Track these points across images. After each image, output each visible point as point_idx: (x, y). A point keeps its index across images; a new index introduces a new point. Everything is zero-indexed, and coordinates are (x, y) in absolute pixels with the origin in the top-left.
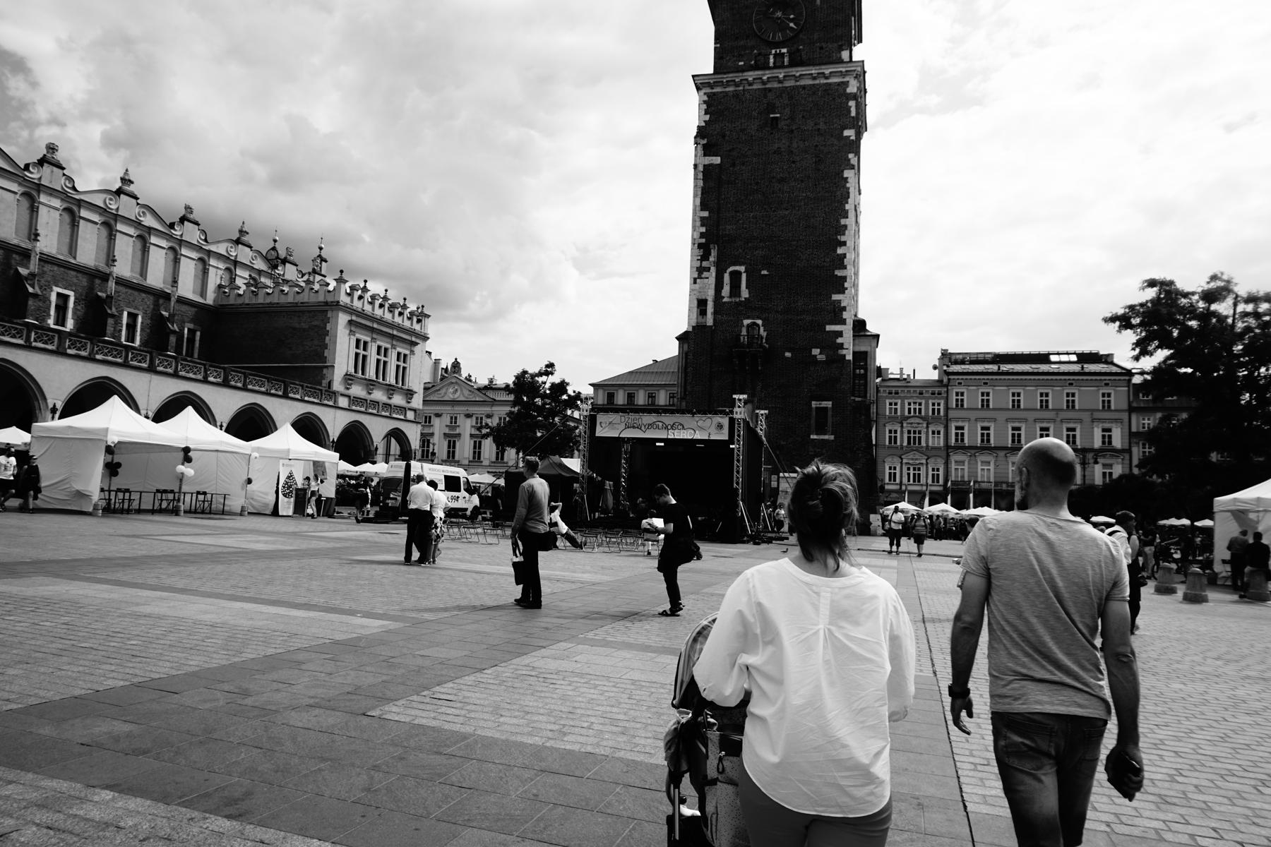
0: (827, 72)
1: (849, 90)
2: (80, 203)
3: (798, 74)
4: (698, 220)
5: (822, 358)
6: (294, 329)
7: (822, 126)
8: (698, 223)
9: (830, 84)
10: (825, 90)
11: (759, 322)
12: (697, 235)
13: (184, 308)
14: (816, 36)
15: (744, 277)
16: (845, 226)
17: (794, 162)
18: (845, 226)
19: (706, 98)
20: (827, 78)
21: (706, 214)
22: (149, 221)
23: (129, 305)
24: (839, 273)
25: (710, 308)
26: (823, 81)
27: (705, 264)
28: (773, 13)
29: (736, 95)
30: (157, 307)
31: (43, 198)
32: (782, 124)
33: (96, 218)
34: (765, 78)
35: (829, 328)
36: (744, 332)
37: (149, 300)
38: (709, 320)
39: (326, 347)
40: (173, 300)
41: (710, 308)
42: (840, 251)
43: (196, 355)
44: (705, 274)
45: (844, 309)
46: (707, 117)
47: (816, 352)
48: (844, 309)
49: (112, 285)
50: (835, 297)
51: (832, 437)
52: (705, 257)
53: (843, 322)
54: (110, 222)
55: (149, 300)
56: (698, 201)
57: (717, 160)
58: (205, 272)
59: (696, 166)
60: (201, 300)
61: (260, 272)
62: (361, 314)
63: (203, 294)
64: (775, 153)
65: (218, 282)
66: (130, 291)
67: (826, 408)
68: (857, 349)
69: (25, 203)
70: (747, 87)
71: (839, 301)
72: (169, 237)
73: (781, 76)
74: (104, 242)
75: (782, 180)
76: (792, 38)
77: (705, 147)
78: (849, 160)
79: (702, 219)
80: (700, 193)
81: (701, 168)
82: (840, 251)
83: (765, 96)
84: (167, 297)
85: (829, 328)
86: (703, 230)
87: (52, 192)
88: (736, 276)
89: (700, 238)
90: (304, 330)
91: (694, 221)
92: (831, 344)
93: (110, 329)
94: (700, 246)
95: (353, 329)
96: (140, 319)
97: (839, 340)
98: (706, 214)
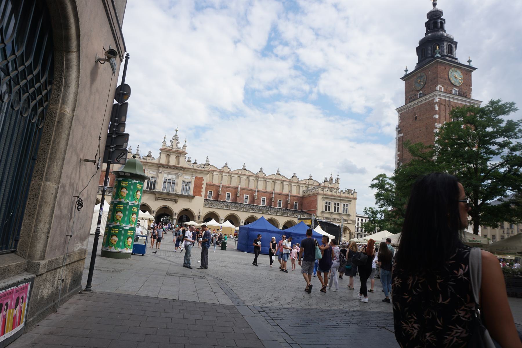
0: (428, 97)
1: (435, 101)
2: (267, 178)
3: (420, 101)
4: (397, 155)
6: (313, 200)
7: (428, 116)
8: (397, 156)
9: (429, 101)
10: (429, 103)
12: (397, 160)
13: (294, 198)
14: (429, 84)
17: (421, 130)
19: (400, 115)
20: (428, 99)
21: (399, 153)
22: (283, 179)
23: (279, 199)
26: (428, 100)
28: (418, 80)
29: (407, 112)
30: (286, 198)
31: (259, 179)
32: (418, 118)
33: (271, 181)
34: (412, 104)
37: (284, 197)
39: (316, 204)
40: (290, 196)
43: (297, 209)
46: (400, 122)
49: (274, 195)
54: (274, 181)
55: (284, 197)
56: (397, 149)
57: (402, 135)
58: (299, 188)
59: (396, 138)
60: (298, 195)
61: (316, 186)
62: (328, 195)
63: (299, 194)
64: (416, 128)
65: (303, 190)
66: (279, 195)
69: (256, 181)
70: (409, 109)
72: (289, 182)
73: (416, 103)
74: (273, 186)
75: (418, 137)
76: (423, 87)
77: (399, 131)
78: (435, 126)
79: (398, 155)
80: (397, 147)
81: (398, 139)
83: (413, 110)
84: (288, 195)
86: (398, 158)
87: (261, 178)
89: (398, 161)
90: (314, 201)
91: (396, 156)
93: (273, 204)
95: (324, 199)
96: (282, 201)
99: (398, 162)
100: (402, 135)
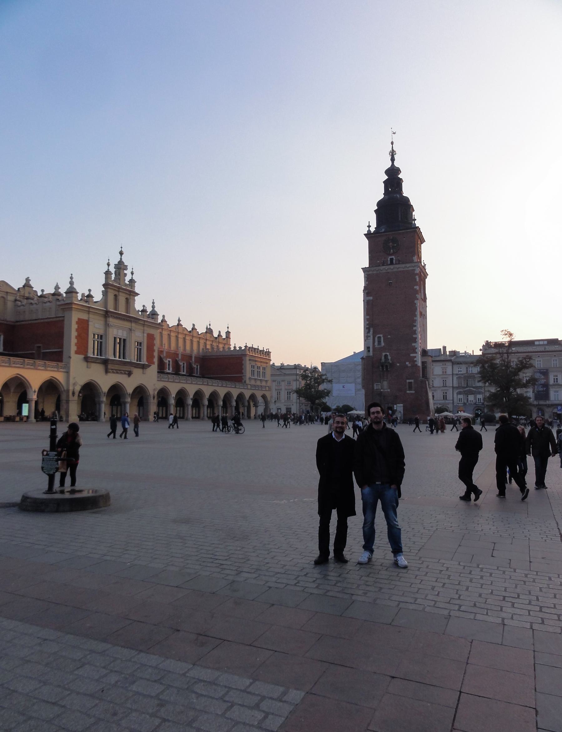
1: (415, 272)
5: (409, 365)
11: (388, 354)
15: (382, 338)
16: (416, 320)
18: (416, 320)
21: (368, 317)
24: (414, 336)
25: (371, 350)
27: (369, 334)
35: (412, 355)
36: (383, 358)
38: (371, 354)
41: (371, 350)
42: (414, 328)
44: (369, 338)
45: (416, 348)
47: (407, 363)
48: (416, 348)
50: (413, 344)
51: (414, 392)
52: (369, 332)
53: (416, 353)
57: (371, 298)
67: (411, 382)
68: (423, 361)
71: (415, 346)
81: (366, 301)
82: (414, 328)
85: (412, 355)
86: (368, 323)
88: (379, 338)
92: (413, 360)
94: (367, 328)
97: (415, 359)
98: (368, 317)
99: (368, 326)
100: (371, 298)
